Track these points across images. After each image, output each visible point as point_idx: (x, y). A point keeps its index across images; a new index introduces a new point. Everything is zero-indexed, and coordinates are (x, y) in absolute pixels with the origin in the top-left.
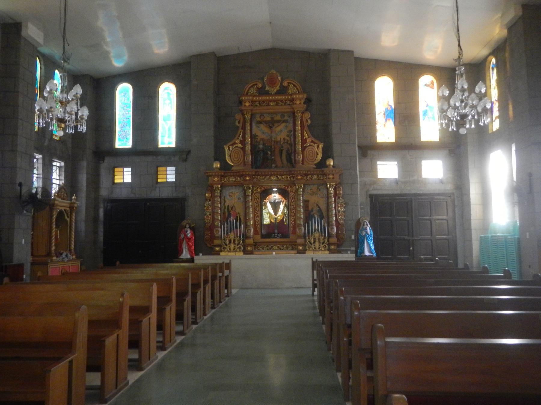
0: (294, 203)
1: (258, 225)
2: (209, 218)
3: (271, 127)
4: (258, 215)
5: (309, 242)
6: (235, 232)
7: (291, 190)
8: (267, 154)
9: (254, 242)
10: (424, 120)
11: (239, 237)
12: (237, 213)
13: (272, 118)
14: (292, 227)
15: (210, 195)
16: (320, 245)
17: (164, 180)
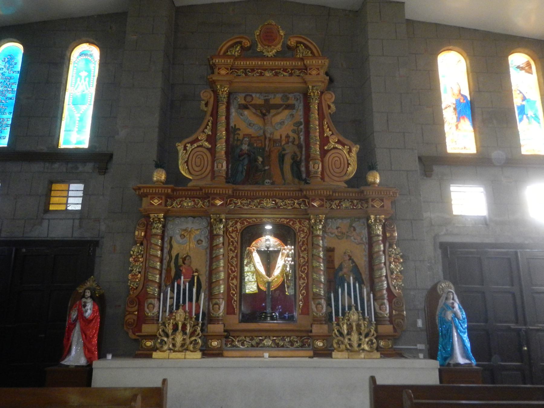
0: (306, 252)
1: (234, 295)
2: (137, 278)
4: (234, 275)
5: (338, 331)
6: (187, 309)
7: (300, 227)
8: (256, 160)
9: (225, 331)
11: (194, 320)
12: (194, 270)
13: (267, 101)
14: (301, 301)
15: (143, 234)
16: (360, 340)
17: (62, 208)
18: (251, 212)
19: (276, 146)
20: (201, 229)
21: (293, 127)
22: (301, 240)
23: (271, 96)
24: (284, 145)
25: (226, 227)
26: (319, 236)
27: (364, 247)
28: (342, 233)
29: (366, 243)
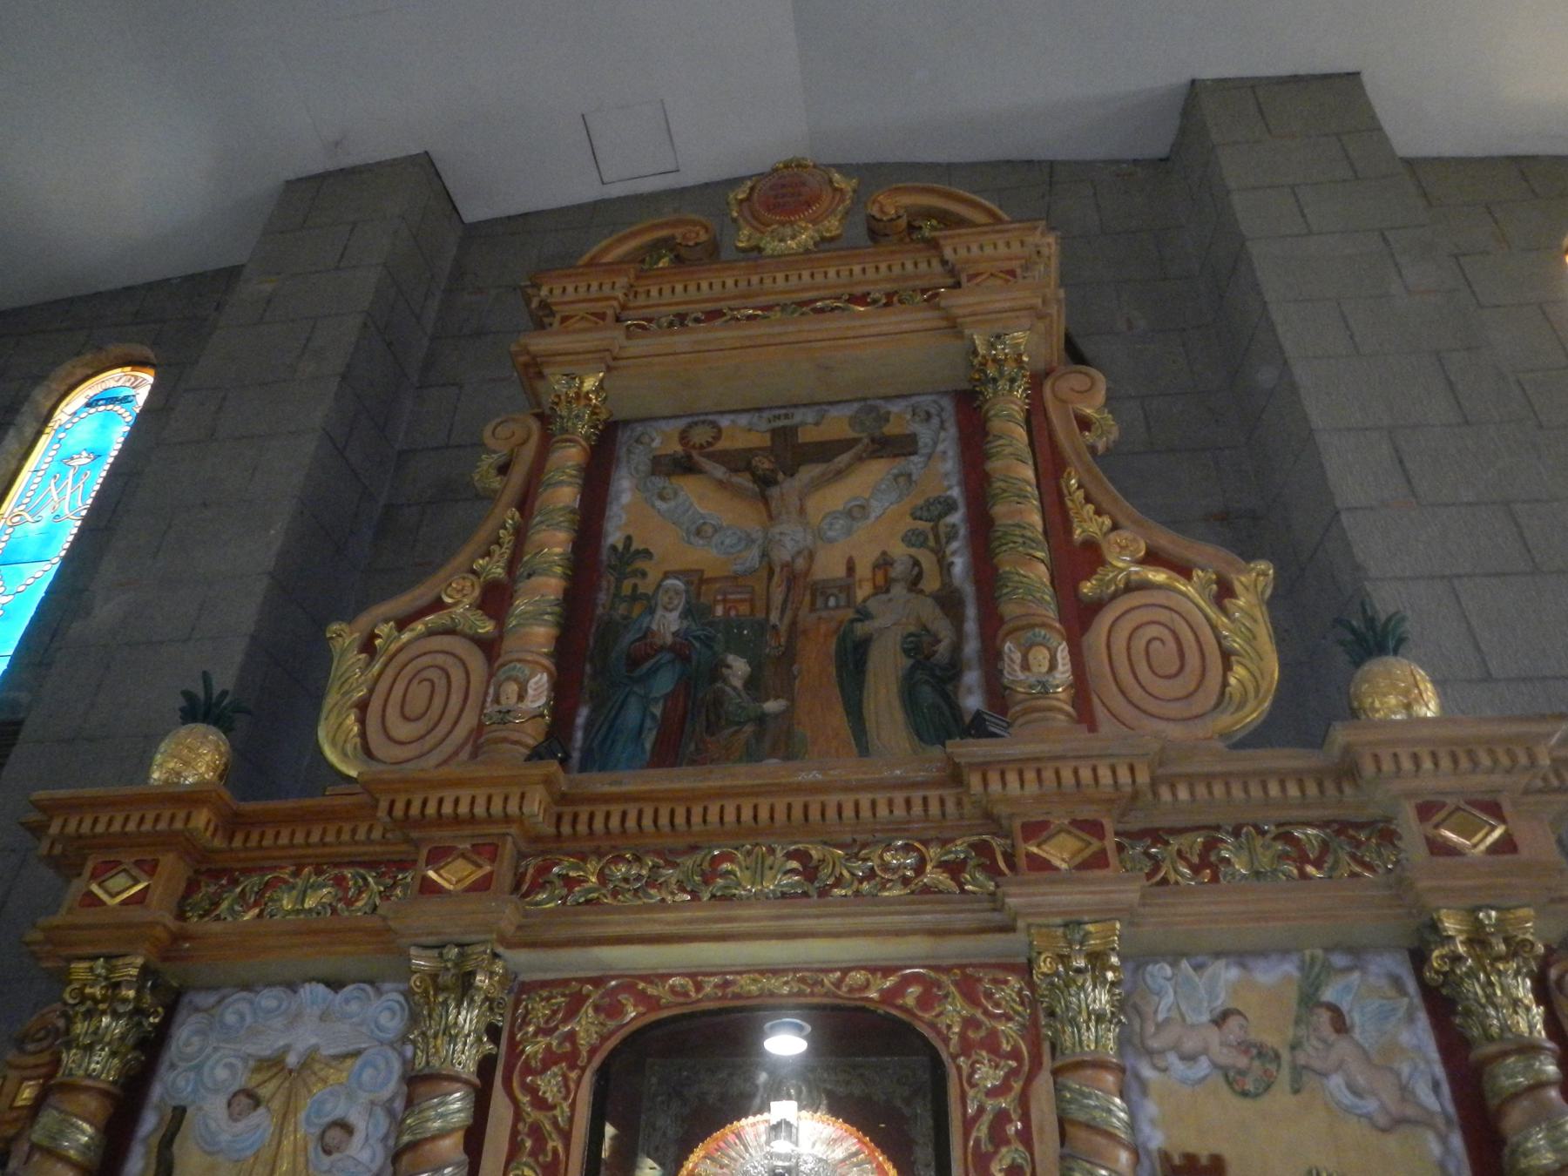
8: (716, 671)
18: (657, 929)
19: (826, 607)
20: (356, 1054)
21: (908, 523)
22: (981, 1110)
23: (799, 415)
24: (865, 601)
25: (512, 1036)
26: (1100, 1065)
27: (1436, 1149)
28: (1260, 1055)
29: (1448, 1121)
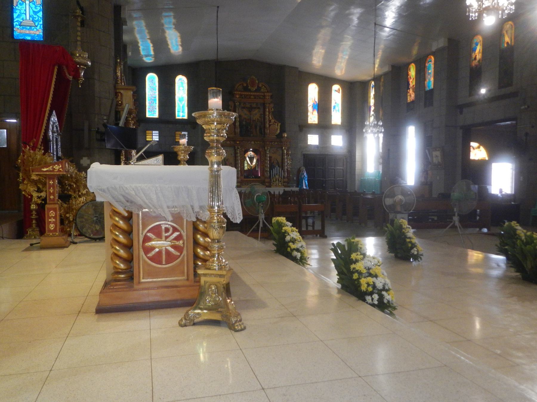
3: (250, 112)
5: (273, 181)
10: (333, 111)
13: (251, 106)
16: (279, 183)
